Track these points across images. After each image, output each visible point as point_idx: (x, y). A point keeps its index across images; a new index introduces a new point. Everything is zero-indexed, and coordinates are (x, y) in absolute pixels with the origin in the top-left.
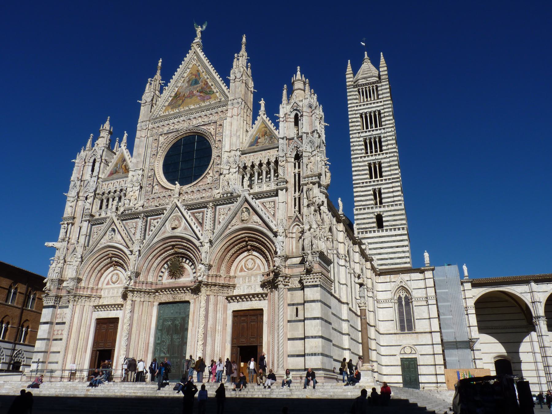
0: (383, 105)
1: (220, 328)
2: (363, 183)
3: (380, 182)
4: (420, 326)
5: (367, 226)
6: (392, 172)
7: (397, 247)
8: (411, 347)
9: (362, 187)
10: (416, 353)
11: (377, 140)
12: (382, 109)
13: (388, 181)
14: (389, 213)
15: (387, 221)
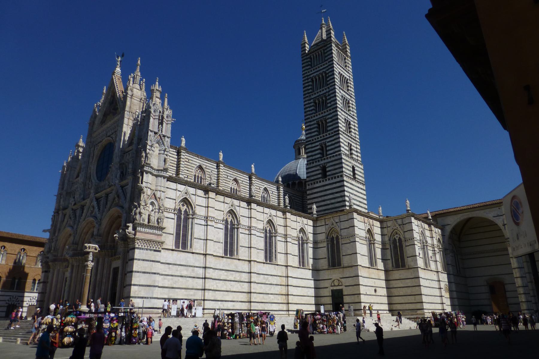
0: (327, 67)
1: (105, 281)
2: (313, 140)
3: (325, 137)
4: (345, 261)
5: (315, 177)
6: (334, 126)
7: (337, 193)
8: (338, 280)
9: (312, 144)
10: (342, 285)
11: (324, 98)
12: (327, 70)
13: (331, 135)
14: (331, 164)
15: (330, 171)
